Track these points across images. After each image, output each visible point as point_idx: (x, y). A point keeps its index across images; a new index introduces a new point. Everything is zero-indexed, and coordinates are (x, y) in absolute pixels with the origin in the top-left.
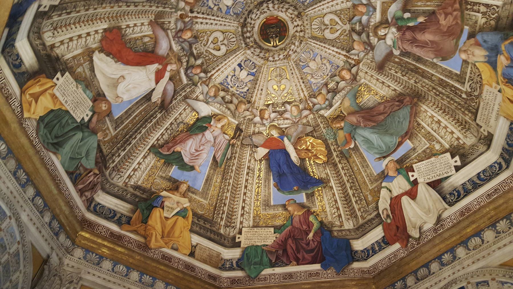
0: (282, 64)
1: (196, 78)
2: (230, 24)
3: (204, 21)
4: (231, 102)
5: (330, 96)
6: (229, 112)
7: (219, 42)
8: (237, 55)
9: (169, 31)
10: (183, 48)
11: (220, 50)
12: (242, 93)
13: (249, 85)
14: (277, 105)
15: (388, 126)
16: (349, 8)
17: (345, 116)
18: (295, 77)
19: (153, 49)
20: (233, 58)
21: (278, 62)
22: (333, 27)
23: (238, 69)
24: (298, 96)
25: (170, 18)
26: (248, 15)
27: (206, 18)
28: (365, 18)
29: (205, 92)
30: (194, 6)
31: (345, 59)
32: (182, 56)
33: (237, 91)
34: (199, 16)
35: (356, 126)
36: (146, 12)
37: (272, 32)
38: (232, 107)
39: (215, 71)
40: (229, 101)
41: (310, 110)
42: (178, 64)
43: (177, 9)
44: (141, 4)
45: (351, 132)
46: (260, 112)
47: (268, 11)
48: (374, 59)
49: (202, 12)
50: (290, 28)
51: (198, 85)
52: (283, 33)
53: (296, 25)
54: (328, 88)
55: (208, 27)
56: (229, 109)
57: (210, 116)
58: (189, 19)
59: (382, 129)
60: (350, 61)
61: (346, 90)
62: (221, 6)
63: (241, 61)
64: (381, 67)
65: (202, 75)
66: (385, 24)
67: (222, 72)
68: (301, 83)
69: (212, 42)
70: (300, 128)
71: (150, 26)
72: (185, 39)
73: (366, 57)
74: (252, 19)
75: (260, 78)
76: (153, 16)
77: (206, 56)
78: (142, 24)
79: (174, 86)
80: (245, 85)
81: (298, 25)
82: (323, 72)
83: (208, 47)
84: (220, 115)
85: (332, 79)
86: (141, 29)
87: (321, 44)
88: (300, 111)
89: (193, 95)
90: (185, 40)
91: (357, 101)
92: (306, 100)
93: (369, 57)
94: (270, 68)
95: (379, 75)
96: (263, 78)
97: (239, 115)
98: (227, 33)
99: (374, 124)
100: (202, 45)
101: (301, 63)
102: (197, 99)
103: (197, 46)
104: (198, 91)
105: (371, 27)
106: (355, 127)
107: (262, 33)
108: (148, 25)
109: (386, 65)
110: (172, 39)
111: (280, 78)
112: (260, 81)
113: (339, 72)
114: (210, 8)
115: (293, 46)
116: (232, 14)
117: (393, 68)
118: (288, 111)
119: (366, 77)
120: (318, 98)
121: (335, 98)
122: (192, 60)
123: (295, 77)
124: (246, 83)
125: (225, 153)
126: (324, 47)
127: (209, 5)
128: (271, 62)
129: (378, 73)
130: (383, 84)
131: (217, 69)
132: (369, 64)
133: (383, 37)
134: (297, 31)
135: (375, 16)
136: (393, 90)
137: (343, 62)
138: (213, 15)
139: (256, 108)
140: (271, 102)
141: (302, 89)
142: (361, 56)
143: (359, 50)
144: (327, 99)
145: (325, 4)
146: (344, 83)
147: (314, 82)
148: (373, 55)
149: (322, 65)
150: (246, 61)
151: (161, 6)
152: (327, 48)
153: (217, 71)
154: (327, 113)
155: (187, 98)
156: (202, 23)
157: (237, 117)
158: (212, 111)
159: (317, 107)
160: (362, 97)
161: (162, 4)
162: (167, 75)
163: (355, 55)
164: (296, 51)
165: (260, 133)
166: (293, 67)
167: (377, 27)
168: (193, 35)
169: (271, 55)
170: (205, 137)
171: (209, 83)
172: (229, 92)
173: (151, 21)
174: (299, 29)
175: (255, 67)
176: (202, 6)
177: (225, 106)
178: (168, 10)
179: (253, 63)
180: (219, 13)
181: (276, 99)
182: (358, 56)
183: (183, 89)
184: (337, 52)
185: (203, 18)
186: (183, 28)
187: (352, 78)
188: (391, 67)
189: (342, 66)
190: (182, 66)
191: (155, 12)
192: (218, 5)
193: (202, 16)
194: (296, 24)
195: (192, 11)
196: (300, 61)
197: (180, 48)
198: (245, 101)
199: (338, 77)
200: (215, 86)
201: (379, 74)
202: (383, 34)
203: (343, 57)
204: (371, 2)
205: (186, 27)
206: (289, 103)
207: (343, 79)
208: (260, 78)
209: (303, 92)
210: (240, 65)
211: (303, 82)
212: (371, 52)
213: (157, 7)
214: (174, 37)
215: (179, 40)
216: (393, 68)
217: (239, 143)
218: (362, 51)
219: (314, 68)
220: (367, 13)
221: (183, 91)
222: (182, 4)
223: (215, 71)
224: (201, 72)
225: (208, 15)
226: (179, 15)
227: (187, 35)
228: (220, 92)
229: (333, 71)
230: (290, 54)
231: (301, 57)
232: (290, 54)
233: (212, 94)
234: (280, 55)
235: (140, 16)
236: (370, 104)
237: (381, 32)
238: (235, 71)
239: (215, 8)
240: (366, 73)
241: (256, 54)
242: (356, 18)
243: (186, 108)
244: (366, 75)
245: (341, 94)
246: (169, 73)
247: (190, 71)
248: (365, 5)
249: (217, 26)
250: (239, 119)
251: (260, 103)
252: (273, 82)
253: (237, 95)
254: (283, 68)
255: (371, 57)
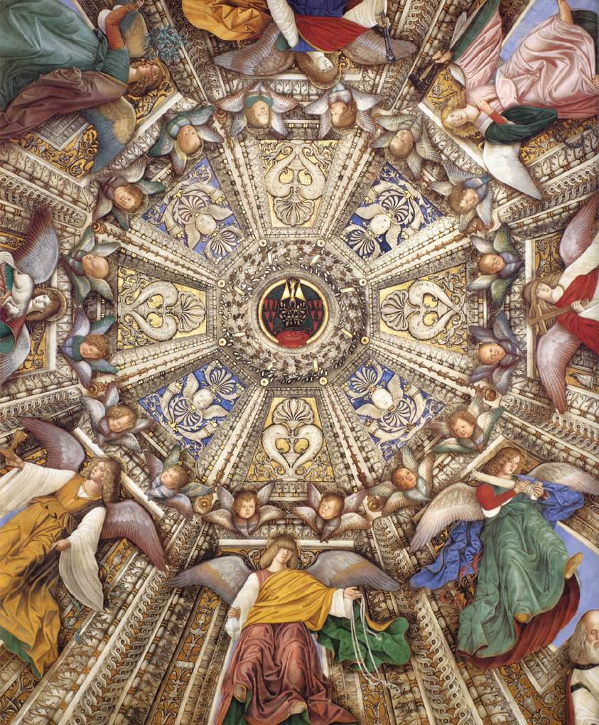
0: (282, 232)
1: (498, 245)
2: (390, 348)
3: (445, 369)
4: (424, 162)
5: (166, 147)
6: (437, 138)
7: (421, 315)
8: (387, 272)
9: (530, 374)
10: (510, 327)
11: (426, 294)
12: (391, 180)
13: (371, 195)
14: (306, 133)
15: (9, 76)
16: (119, 350)
17: (125, 95)
18: (252, 199)
19: (579, 352)
20: (397, 267)
21: (292, 238)
22: (156, 310)
23: (392, 241)
24: (249, 150)
25: (519, 401)
26: (343, 359)
27: (439, 373)
28: (83, 330)
29: (486, 204)
30: (458, 409)
31: (128, 235)
32: (516, 309)
33: (404, 187)
34: (453, 385)
35: (94, 70)
36: (567, 435)
37: (296, 314)
38: (425, 150)
39: (449, 248)
40: (427, 167)
41: (220, 109)
42: (533, 297)
43: (497, 415)
44: (571, 459)
45: (108, 53)
46: (353, 123)
47: (300, 359)
48: (59, 236)
49: (444, 391)
50: (254, 313)
51: (500, 224)
52: (271, 304)
53: (239, 320)
54: (170, 165)
55: (440, 354)
56: (434, 146)
57: (489, 141)
58: (476, 384)
59: (25, 66)
60: (117, 230)
61: (124, 161)
62: (401, 392)
63: (380, 255)
64: (40, 216)
65: (482, 247)
66: (35, 322)
67: (431, 240)
68: (238, 181)
69: (439, 319)
70: (249, 67)
71: (569, 402)
72: (499, 345)
73: (77, 238)
74: (338, 348)
75: (340, 208)
76: (554, 420)
77: (461, 288)
78: (583, 414)
79: (559, 244)
80: (382, 198)
81: (235, 318)
82: (181, 206)
83: (450, 309)
84: (459, 137)
85: (161, 189)
86: (590, 407)
87: (184, 271)
88: (246, 109)
89: (518, 204)
90: (499, 342)
91: (95, 133)
92: (228, 137)
93: (71, 239)
94: (312, 228)
95: (43, 196)
96: (334, 206)
97: (412, 125)
98: (398, 328)
99: (47, 77)
100: (463, 319)
101: (236, 230)
102: (512, 192)
103: (476, 320)
104: (503, 211)
105: (69, 313)
106: (100, 65)
107: (320, 314)
108: (571, 407)
109: (28, 222)
110: (529, 356)
111: (291, 201)
112: (341, 199)
113: (142, 204)
114: (424, 395)
115: (252, 270)
116: (379, 368)
117: (10, 216)
118: (278, 114)
119: (75, 191)
120: (198, 142)
121: (153, 142)
122: (495, 292)
123: (252, 199)
124: (377, 202)
125: (472, 31)
126: (177, 264)
127: (425, 401)
128: (308, 240)
129: (47, 203)
130: (31, 175)
131: (442, 251)
132: (69, 222)
133: (39, 290)
134: (240, 305)
135: (58, 335)
136: (6, 162)
137: (134, 227)
138: (422, 376)
139: (364, 135)
140: (320, 143)
141: (238, 167)
142: (91, 242)
143: (96, 256)
144: (175, 138)
145: (171, 361)
146: (130, 177)
147: (206, 182)
148: (61, 244)
149: (185, 222)
150: (369, 255)
151: (530, 433)
152: (172, 261)
153: (444, 245)
154: (176, 101)
155: (536, 200)
156: (452, 366)
157: (419, 120)
158: (482, 152)
159: (200, 120)
160: (83, 143)
161: (527, 440)
162: (567, 279)
163: (105, 244)
164: (246, 261)
165: (364, 67)
166: (256, 222)
167: (55, 311)
168: (478, 346)
169: (306, 257)
170: (517, 90)
171: (471, 222)
172: (426, 189)
173: (562, 412)
174: (235, 310)
175: (349, 236)
176: (441, 403)
177: (443, 157)
178: (518, 421)
179: (352, 247)
180: (406, 374)
181: (306, 150)
182: (96, 241)
183: (538, 229)
184: (148, 250)
185: (445, 376)
186: (497, 370)
187: (110, 191)
188: (16, 218)
189: (136, 219)
190: (525, 287)
191: (546, 426)
192: (405, 397)
193: (447, 382)
194: (240, 322)
195: (467, 399)
196: (237, 237)
197: (517, 331)
198: (388, 157)
199: (146, 193)
200: (458, 214)
201: (45, 199)
202: (40, 298)
203: (135, 238)
204: (70, 365)
205: (487, 370)
206: (272, 134)
207: (133, 188)
208: (340, 208)
209: (235, 160)
210: (385, 247)
211: (233, 183)
212: (66, 253)
213: (538, 436)
214: (523, 358)
215: (514, 349)
216: (10, 216)
217: (427, 48)
218: (86, 253)
219: (206, 217)
220: (78, 341)
221: (540, 223)
222: (484, 421)
223: (449, 248)
224: (483, 255)
225: (432, 380)
226: (497, 401)
227: (490, 351)
228: (447, 194)
229: (157, 208)
230: (261, 255)
231: (234, 244)
232: (261, 255)
233: (469, 194)
234: (285, 255)
235: (582, 431)
236: (60, 128)
237: (43, 301)
238: (400, 235)
239: (413, 390)
240: (75, 202)
241: (341, 267)
242: (102, 329)
243: (546, 178)
244: (75, 196)
245: (136, 150)
246: (560, 282)
247: (508, 266)
248: (83, 359)
249: (418, 350)
250: (414, 114)
251: (349, 145)
252: (308, 192)
253: (406, 177)
254: (280, 225)
255: (65, 240)
